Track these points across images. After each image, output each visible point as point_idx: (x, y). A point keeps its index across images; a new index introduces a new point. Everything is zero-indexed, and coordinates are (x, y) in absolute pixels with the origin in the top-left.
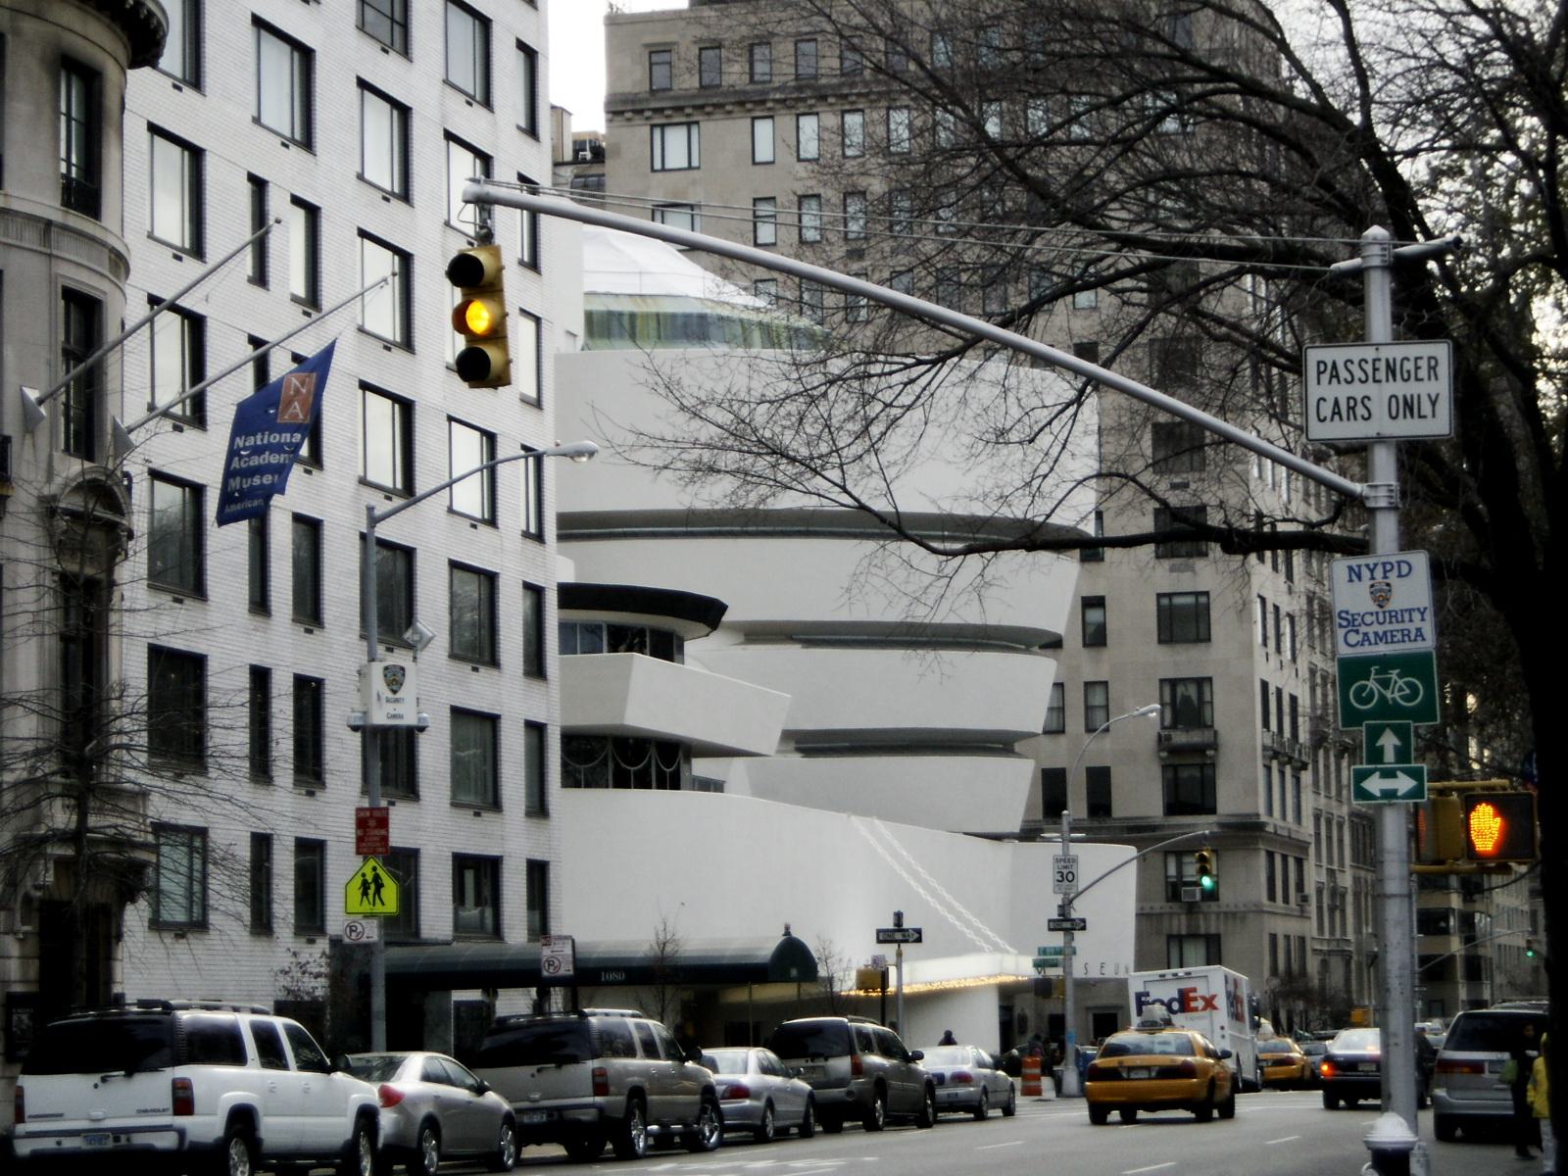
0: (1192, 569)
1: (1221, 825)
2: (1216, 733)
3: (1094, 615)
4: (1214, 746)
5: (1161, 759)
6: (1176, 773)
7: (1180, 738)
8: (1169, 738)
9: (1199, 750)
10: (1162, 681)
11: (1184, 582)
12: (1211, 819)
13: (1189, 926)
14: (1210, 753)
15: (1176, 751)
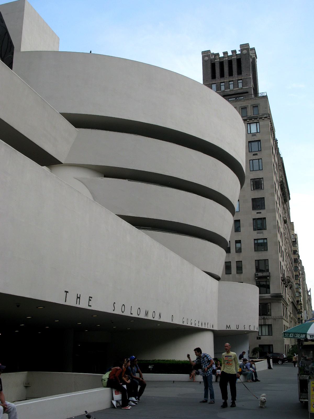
0: (262, 233)
1: (272, 296)
2: (270, 273)
3: (238, 245)
4: (269, 276)
5: (256, 280)
6: (259, 282)
7: (260, 274)
8: (258, 274)
9: (266, 277)
10: (255, 260)
11: (260, 236)
12: (269, 295)
13: (264, 322)
14: (268, 278)
15: (260, 278)
